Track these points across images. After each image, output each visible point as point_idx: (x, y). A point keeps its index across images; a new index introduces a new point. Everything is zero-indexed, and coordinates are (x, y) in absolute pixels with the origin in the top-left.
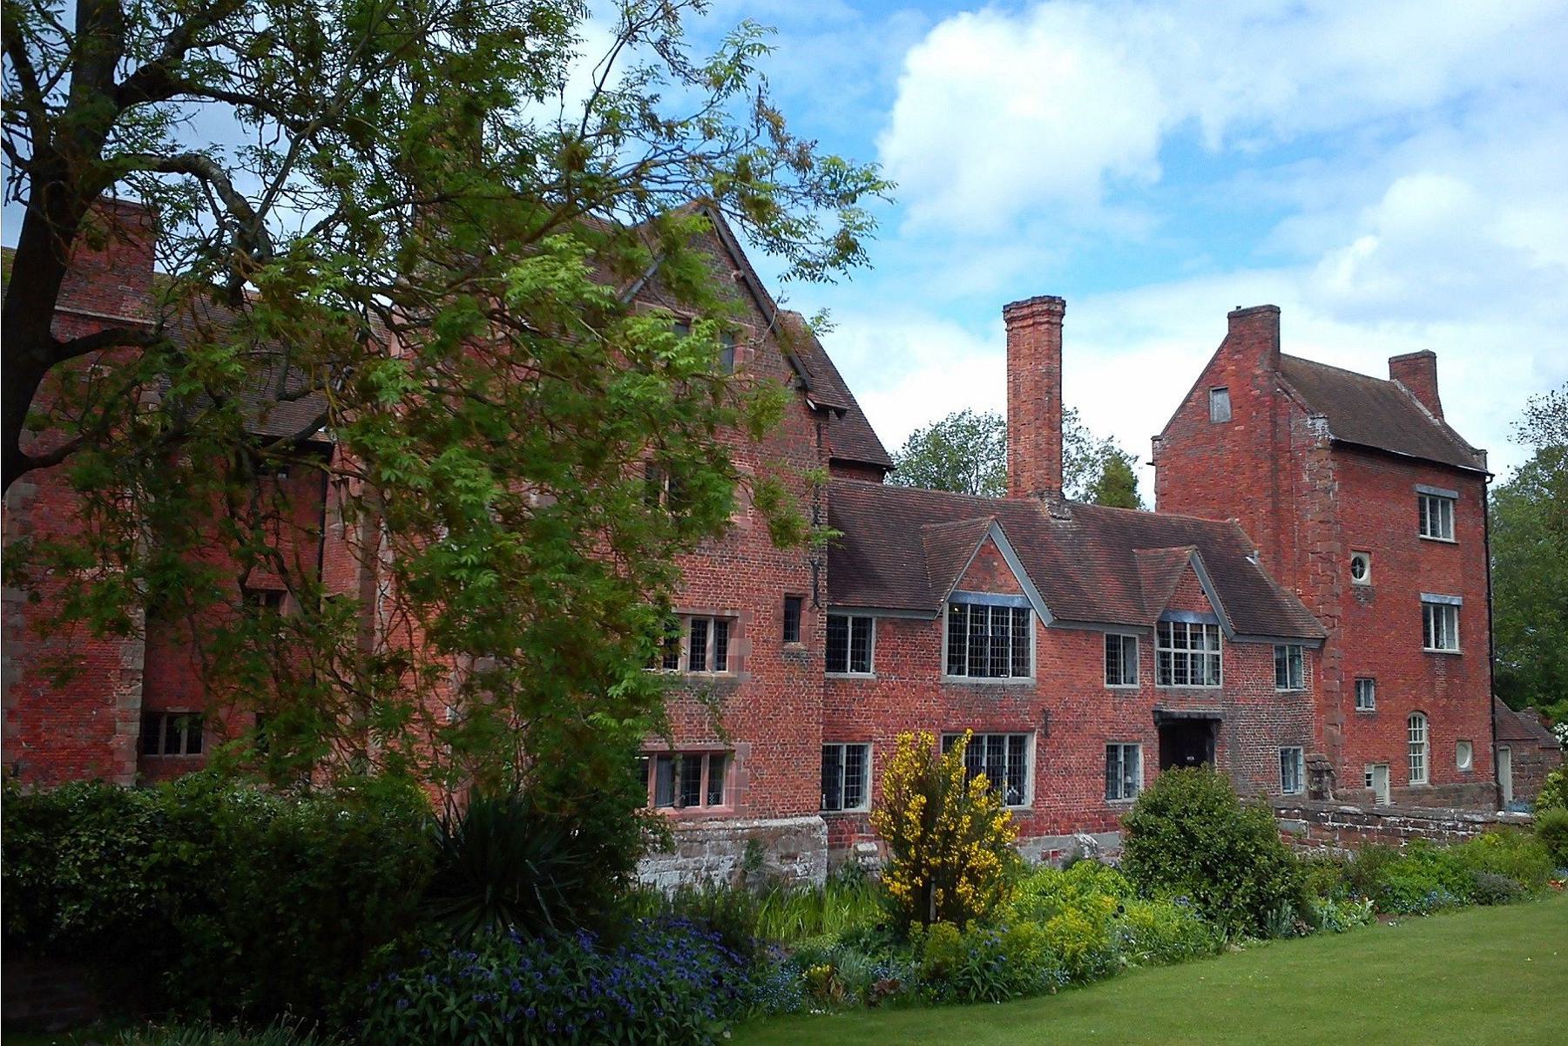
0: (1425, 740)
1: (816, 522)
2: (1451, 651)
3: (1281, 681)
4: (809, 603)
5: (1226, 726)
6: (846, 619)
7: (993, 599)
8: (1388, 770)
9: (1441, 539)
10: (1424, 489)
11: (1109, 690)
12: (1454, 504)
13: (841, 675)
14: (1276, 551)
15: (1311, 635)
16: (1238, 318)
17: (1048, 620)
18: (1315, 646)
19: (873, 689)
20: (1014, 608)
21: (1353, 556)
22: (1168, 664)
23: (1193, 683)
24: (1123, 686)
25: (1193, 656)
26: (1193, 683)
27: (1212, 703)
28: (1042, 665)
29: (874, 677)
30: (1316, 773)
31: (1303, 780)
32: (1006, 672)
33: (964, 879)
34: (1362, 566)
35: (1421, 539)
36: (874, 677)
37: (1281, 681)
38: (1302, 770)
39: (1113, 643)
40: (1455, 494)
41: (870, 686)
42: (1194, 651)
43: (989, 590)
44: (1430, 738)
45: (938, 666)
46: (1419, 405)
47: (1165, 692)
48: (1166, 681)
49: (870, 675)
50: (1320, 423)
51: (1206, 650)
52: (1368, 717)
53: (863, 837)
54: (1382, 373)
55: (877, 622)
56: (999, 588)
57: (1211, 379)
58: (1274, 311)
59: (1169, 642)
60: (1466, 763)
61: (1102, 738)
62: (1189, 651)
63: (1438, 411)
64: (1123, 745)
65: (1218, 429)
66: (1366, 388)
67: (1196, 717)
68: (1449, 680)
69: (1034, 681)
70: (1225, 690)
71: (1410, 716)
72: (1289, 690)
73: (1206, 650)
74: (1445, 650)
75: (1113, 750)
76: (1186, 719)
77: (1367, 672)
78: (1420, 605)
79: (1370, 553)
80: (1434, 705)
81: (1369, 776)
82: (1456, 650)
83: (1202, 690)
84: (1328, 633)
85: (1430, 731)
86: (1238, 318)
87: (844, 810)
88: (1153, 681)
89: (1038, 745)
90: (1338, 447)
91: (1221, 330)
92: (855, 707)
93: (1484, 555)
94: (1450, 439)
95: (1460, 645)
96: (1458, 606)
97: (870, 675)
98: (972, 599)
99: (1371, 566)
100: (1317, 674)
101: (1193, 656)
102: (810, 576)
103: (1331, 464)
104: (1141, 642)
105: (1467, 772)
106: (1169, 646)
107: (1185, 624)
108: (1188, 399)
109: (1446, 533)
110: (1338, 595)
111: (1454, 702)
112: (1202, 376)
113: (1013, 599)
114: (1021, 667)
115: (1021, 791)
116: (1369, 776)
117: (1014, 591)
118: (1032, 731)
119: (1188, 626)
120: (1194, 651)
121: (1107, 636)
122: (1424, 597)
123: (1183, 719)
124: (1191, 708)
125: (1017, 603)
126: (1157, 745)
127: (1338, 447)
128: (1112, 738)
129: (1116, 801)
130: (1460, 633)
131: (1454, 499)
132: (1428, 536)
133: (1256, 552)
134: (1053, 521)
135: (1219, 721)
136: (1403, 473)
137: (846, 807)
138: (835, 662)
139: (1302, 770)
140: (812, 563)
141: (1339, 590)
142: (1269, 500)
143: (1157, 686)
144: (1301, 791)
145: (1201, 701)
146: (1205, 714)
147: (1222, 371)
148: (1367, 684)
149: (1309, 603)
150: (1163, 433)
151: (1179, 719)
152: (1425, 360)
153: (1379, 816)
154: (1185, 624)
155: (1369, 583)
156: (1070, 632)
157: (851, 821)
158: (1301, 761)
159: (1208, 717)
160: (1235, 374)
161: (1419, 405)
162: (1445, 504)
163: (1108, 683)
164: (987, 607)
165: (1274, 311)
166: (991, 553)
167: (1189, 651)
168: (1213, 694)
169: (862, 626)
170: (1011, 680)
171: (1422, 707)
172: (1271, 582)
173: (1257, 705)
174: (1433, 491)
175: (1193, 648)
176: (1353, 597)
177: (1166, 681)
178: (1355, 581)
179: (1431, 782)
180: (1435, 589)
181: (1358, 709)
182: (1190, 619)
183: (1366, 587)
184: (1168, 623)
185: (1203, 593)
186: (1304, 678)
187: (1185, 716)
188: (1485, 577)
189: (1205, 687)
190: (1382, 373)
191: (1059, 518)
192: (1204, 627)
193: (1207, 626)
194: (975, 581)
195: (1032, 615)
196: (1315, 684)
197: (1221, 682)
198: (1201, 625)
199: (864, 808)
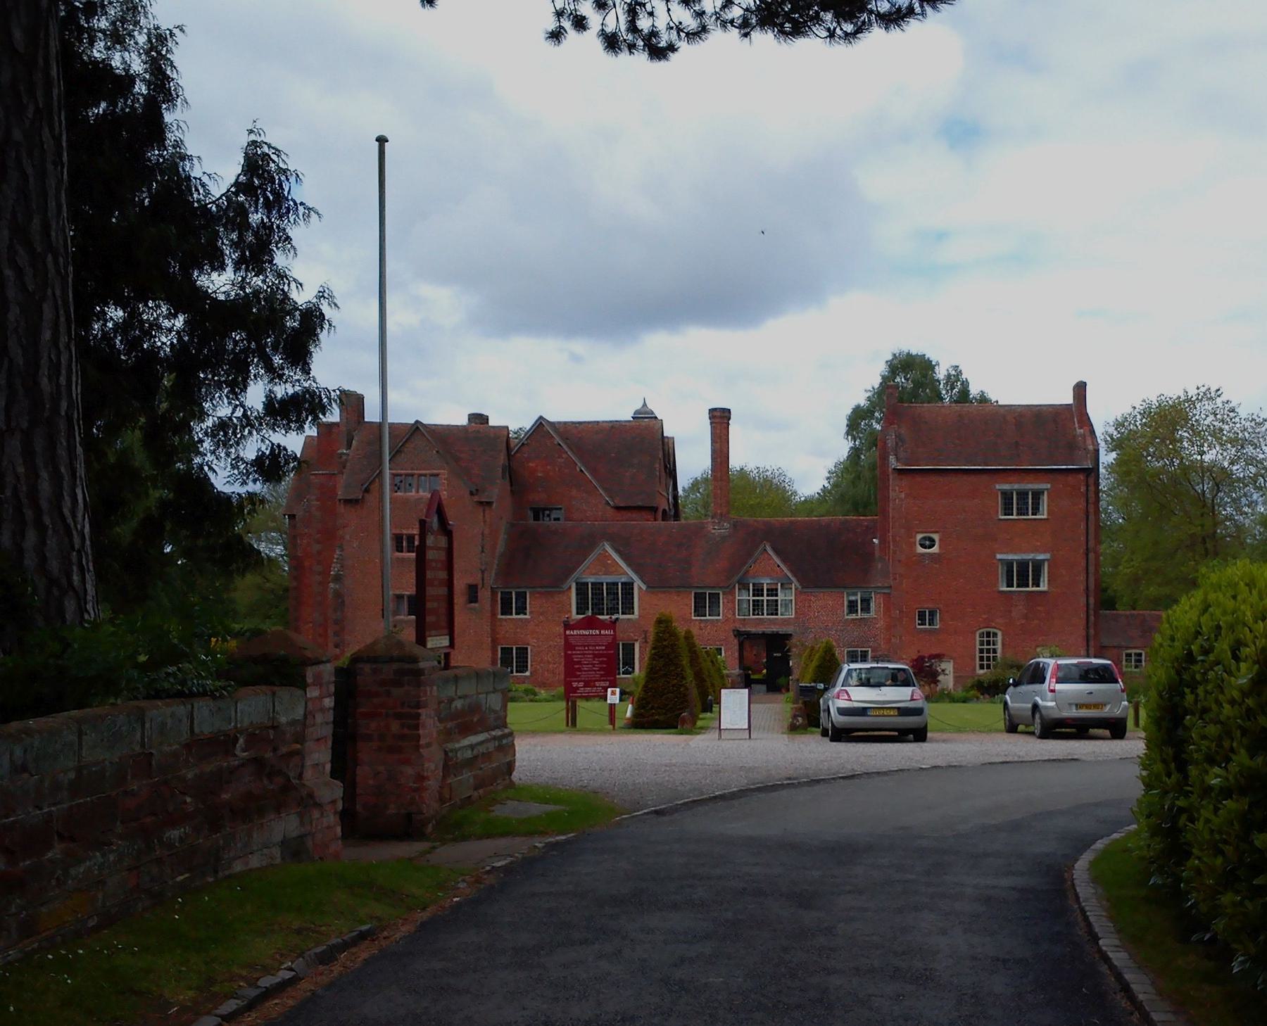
1: (483, 552)
4: (480, 587)
6: (511, 593)
10: (1006, 487)
11: (696, 620)
12: (1048, 493)
17: (644, 587)
19: (529, 622)
21: (919, 536)
23: (768, 615)
24: (708, 618)
26: (768, 615)
32: (618, 613)
34: (932, 540)
40: (1049, 486)
45: (570, 612)
49: (527, 617)
55: (530, 593)
56: (611, 573)
67: (769, 633)
70: (795, 618)
71: (985, 630)
72: (859, 617)
85: (1003, 640)
87: (515, 674)
88: (734, 614)
89: (640, 647)
95: (1049, 584)
97: (527, 617)
98: (591, 580)
99: (940, 540)
102: (480, 575)
107: (763, 584)
111: (1036, 622)
113: (621, 578)
114: (629, 608)
115: (633, 668)
118: (637, 640)
119: (765, 585)
122: (999, 556)
123: (759, 634)
124: (765, 628)
131: (1047, 489)
135: (791, 635)
136: (985, 477)
138: (506, 610)
140: (481, 570)
143: (737, 617)
145: (775, 624)
146: (777, 632)
151: (755, 634)
156: (664, 592)
159: (780, 633)
163: (695, 616)
164: (602, 584)
166: (605, 556)
169: (521, 597)
171: (993, 624)
173: (826, 626)
174: (1016, 486)
178: (920, 550)
182: (766, 582)
184: (749, 584)
185: (779, 566)
187: (760, 633)
188: (1083, 538)
189: (779, 616)
192: (779, 584)
193: (782, 584)
194: (594, 571)
197: (721, 614)
198: (777, 584)
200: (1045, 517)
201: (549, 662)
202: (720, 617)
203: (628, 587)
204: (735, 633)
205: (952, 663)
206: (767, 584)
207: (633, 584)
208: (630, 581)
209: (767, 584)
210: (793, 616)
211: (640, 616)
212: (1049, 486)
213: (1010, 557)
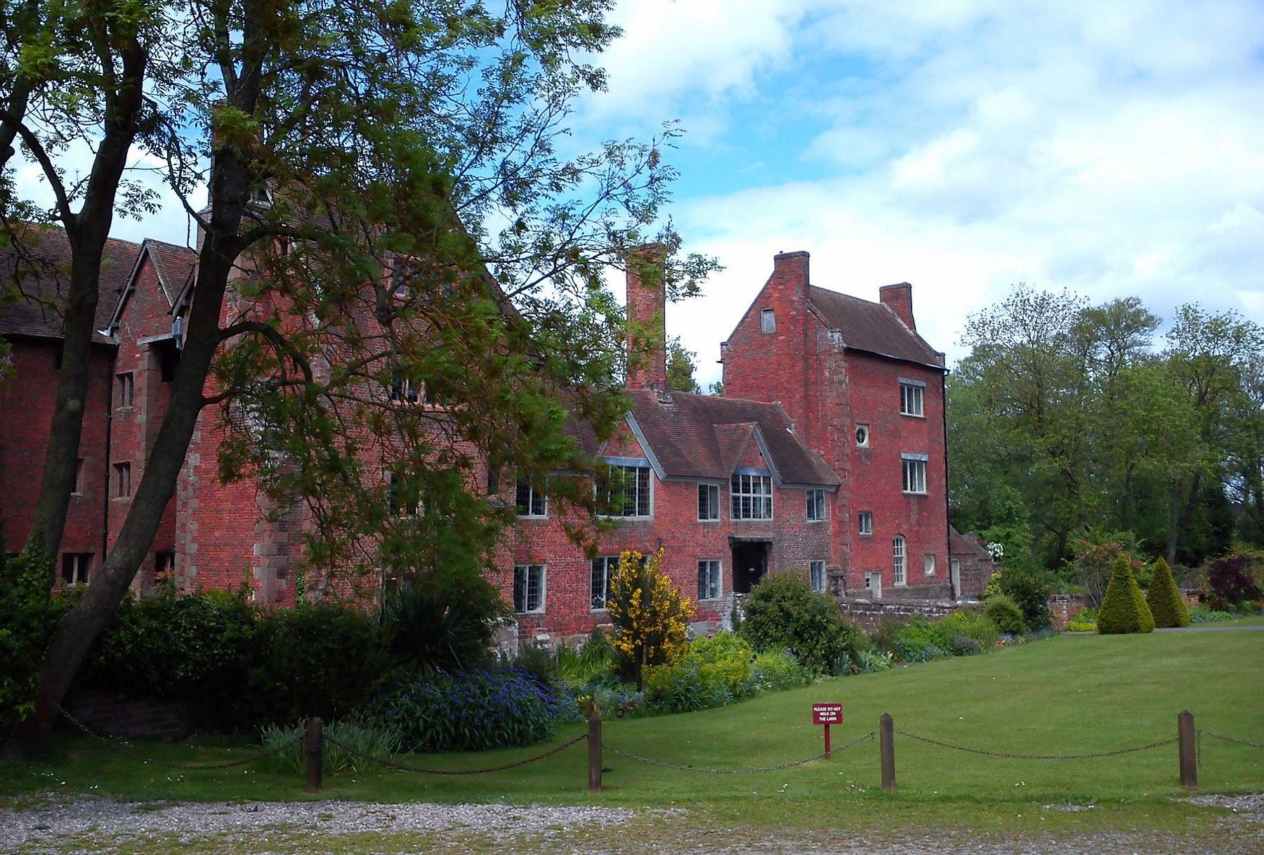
0: (904, 554)
2: (921, 492)
3: (810, 515)
5: (775, 547)
7: (627, 461)
8: (880, 576)
9: (915, 415)
10: (903, 380)
13: (525, 517)
14: (807, 426)
15: (831, 483)
16: (781, 259)
18: (833, 490)
19: (547, 526)
20: (639, 468)
22: (739, 504)
23: (754, 517)
25: (754, 498)
26: (754, 517)
27: (766, 531)
28: (657, 507)
29: (547, 518)
30: (834, 578)
31: (824, 584)
33: (667, 640)
34: (863, 434)
35: (902, 415)
36: (547, 518)
37: (810, 515)
38: (824, 577)
39: (703, 491)
40: (924, 384)
41: (544, 524)
42: (755, 495)
43: (624, 455)
44: (908, 553)
46: (900, 321)
47: (736, 524)
48: (737, 516)
50: (837, 336)
51: (763, 495)
52: (867, 539)
53: (540, 630)
54: (875, 298)
57: (762, 303)
58: (806, 255)
59: (739, 489)
60: (931, 571)
61: (696, 557)
62: (752, 495)
63: (912, 325)
64: (709, 561)
65: (766, 338)
66: (865, 309)
67: (756, 540)
68: (920, 514)
69: (652, 519)
71: (895, 538)
72: (816, 521)
73: (763, 495)
74: (917, 492)
75: (702, 565)
76: (749, 543)
77: (866, 508)
78: (901, 461)
79: (868, 425)
80: (910, 530)
81: (868, 580)
82: (924, 492)
83: (760, 522)
84: (841, 481)
85: (907, 548)
86: (781, 259)
87: (527, 612)
90: (849, 352)
91: (770, 268)
92: (535, 539)
93: (943, 426)
94: (920, 345)
95: (927, 488)
96: (926, 462)
100: (834, 510)
101: (754, 498)
103: (844, 364)
104: (721, 489)
105: (932, 577)
106: (739, 492)
108: (746, 316)
109: (918, 411)
110: (847, 455)
112: (756, 300)
116: (868, 580)
117: (639, 456)
120: (755, 495)
121: (700, 486)
122: (903, 456)
125: (642, 464)
126: (731, 561)
127: (849, 352)
128: (703, 556)
129: (705, 600)
130: (927, 481)
131: (923, 388)
132: (906, 413)
133: (793, 425)
134: (660, 405)
136: (889, 369)
137: (529, 609)
139: (824, 577)
141: (849, 451)
142: (803, 389)
144: (824, 590)
145: (759, 529)
147: (769, 297)
148: (867, 516)
149: (828, 461)
150: (729, 340)
152: (904, 289)
153: (881, 605)
154: (749, 477)
155: (868, 446)
157: (532, 619)
158: (824, 570)
160: (779, 299)
161: (900, 321)
162: (917, 391)
165: (806, 255)
167: (752, 495)
168: (767, 525)
170: (637, 518)
171: (902, 532)
172: (803, 446)
174: (909, 382)
175: (754, 492)
176: (857, 456)
177: (737, 516)
179: (908, 584)
180: (910, 450)
181: (861, 533)
182: (752, 473)
183: (866, 449)
185: (761, 454)
186: (826, 513)
189: (762, 520)
190: (875, 298)
191: (665, 403)
195: (651, 470)
196: (833, 516)
198: (760, 477)
199: (541, 610)
200: (922, 416)
201: (565, 590)
202: (718, 520)
203: (644, 471)
204: (731, 541)
205: (880, 576)
206: (753, 477)
207: (649, 469)
208: (647, 466)
209: (753, 477)
210: (772, 519)
211: (655, 517)
212: (924, 384)
213: (909, 457)
